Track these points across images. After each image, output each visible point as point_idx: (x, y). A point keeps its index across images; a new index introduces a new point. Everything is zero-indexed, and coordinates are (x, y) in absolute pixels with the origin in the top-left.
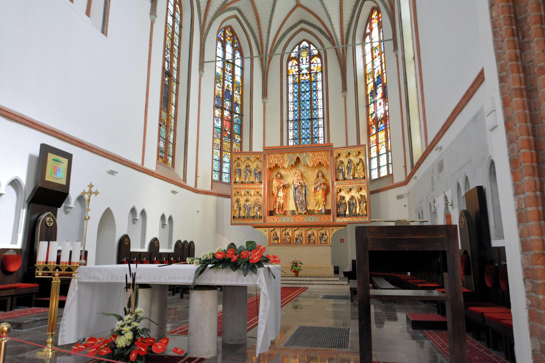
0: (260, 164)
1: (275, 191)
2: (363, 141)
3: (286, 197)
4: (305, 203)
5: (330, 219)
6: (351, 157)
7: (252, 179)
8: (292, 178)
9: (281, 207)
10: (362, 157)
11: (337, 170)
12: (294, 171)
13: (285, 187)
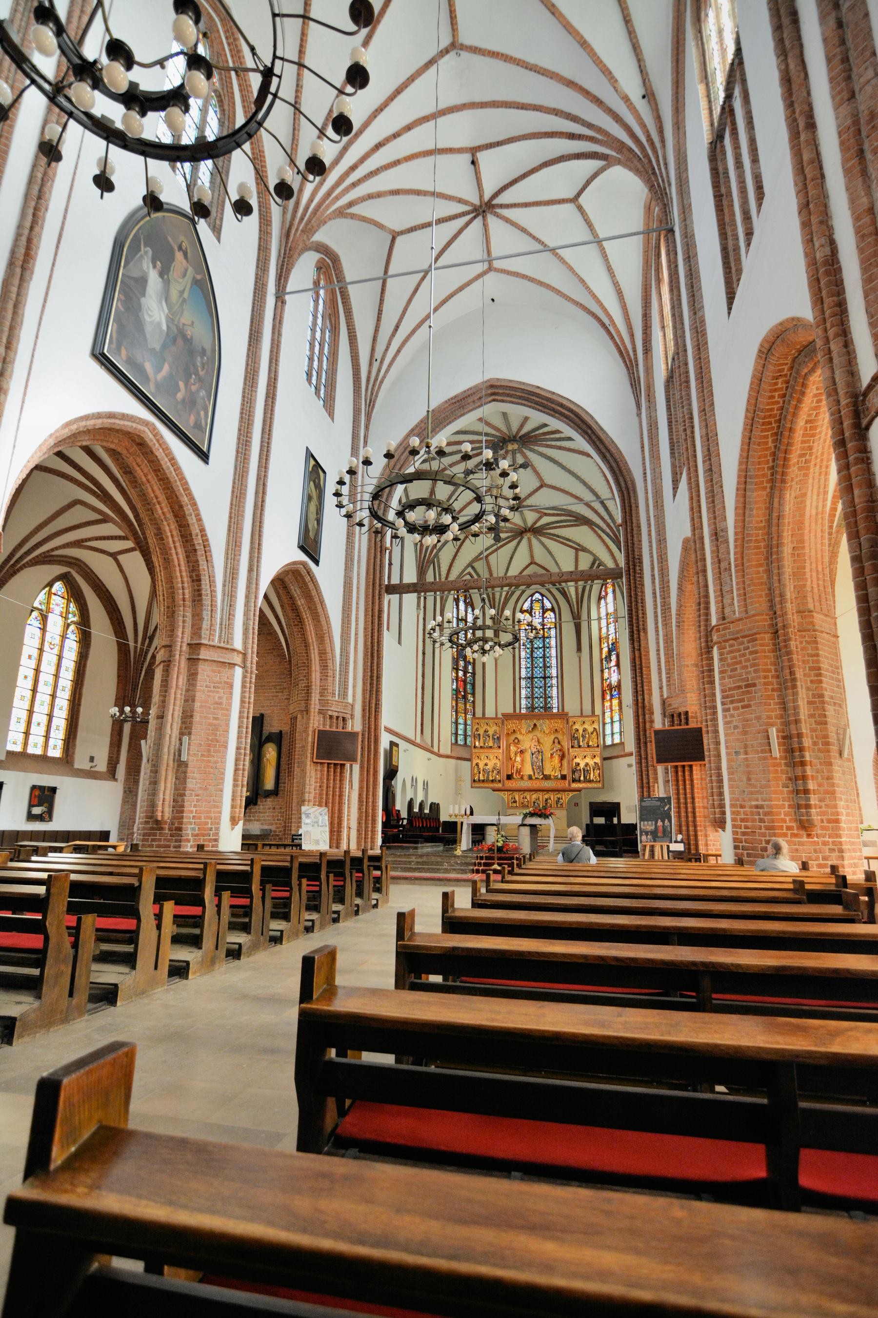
0: (497, 729)
1: (512, 755)
2: (598, 711)
3: (523, 761)
4: (541, 769)
5: (565, 784)
6: (586, 726)
7: (491, 744)
8: (528, 742)
9: (519, 771)
10: (596, 726)
11: (573, 738)
12: (531, 736)
13: (522, 752)
